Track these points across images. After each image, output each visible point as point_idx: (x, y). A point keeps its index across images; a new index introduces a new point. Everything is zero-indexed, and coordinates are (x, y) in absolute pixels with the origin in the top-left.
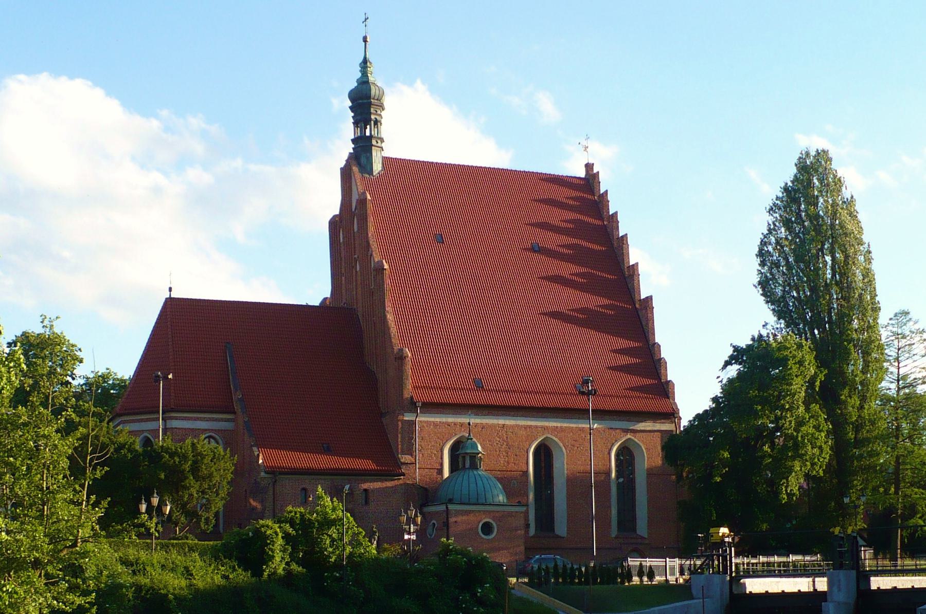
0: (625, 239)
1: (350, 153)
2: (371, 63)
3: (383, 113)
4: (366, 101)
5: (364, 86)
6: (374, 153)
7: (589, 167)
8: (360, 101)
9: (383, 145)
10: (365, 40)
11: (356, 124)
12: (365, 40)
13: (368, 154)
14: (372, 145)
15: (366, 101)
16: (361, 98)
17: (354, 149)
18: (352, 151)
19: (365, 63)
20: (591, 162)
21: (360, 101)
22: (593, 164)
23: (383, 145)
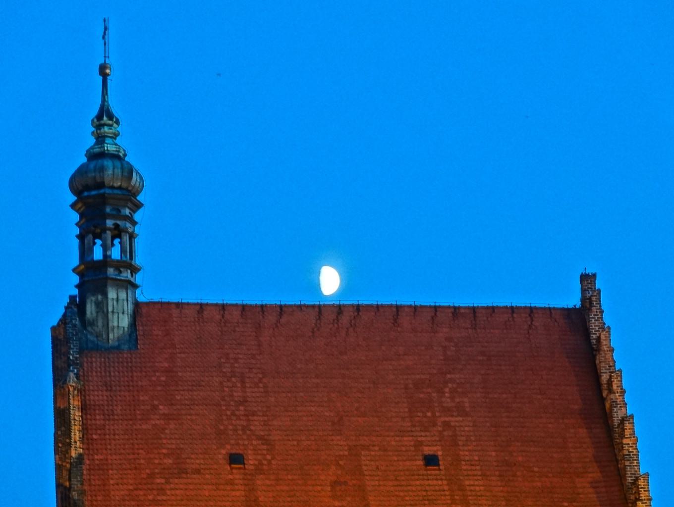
0: (627, 425)
1: (72, 298)
2: (111, 117)
3: (137, 216)
4: (94, 193)
5: (92, 165)
6: (112, 294)
7: (587, 280)
8: (86, 194)
9: (138, 279)
10: (103, 71)
11: (81, 237)
12: (103, 71)
13: (100, 297)
14: (107, 278)
15: (94, 193)
16: (87, 188)
17: (78, 286)
18: (75, 292)
19: (104, 114)
20: (590, 271)
21: (86, 194)
22: (594, 275)
23: (138, 279)
